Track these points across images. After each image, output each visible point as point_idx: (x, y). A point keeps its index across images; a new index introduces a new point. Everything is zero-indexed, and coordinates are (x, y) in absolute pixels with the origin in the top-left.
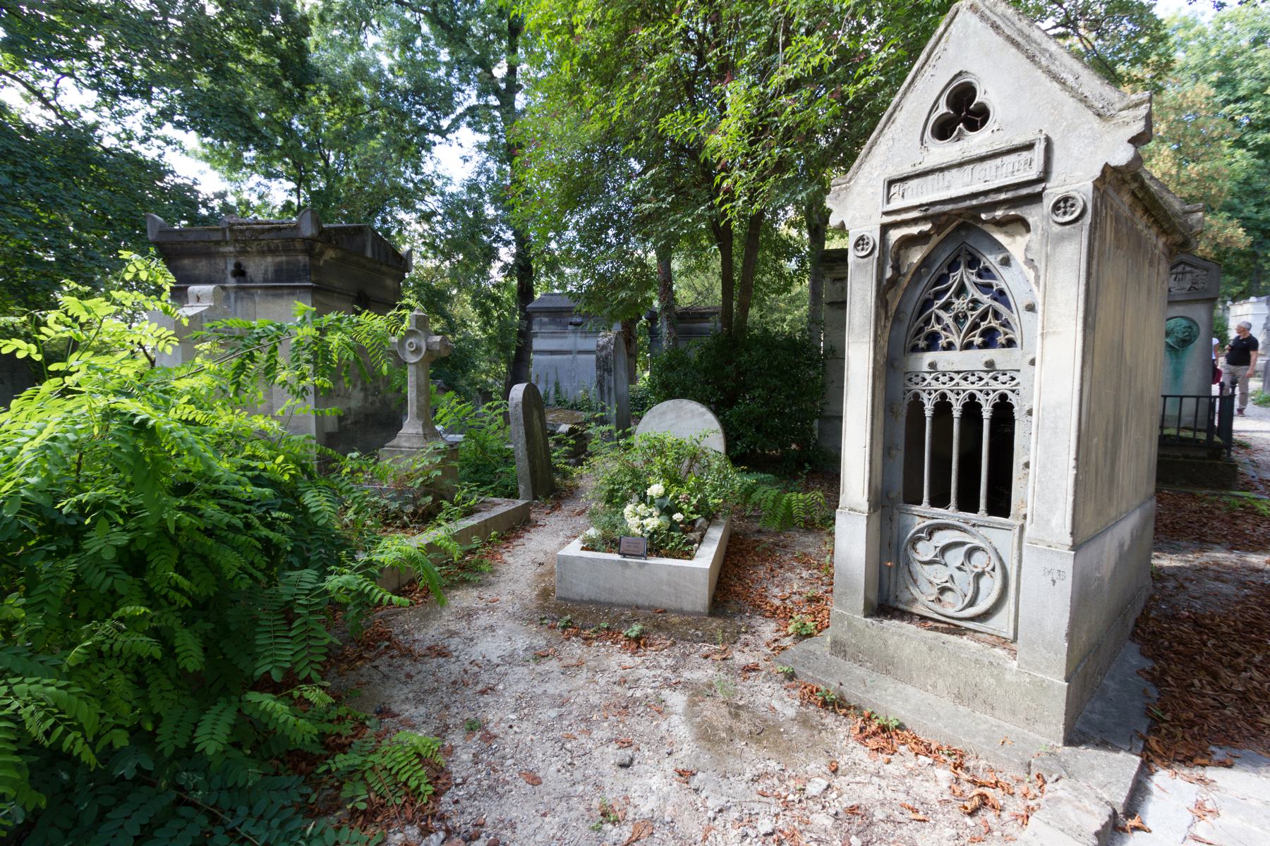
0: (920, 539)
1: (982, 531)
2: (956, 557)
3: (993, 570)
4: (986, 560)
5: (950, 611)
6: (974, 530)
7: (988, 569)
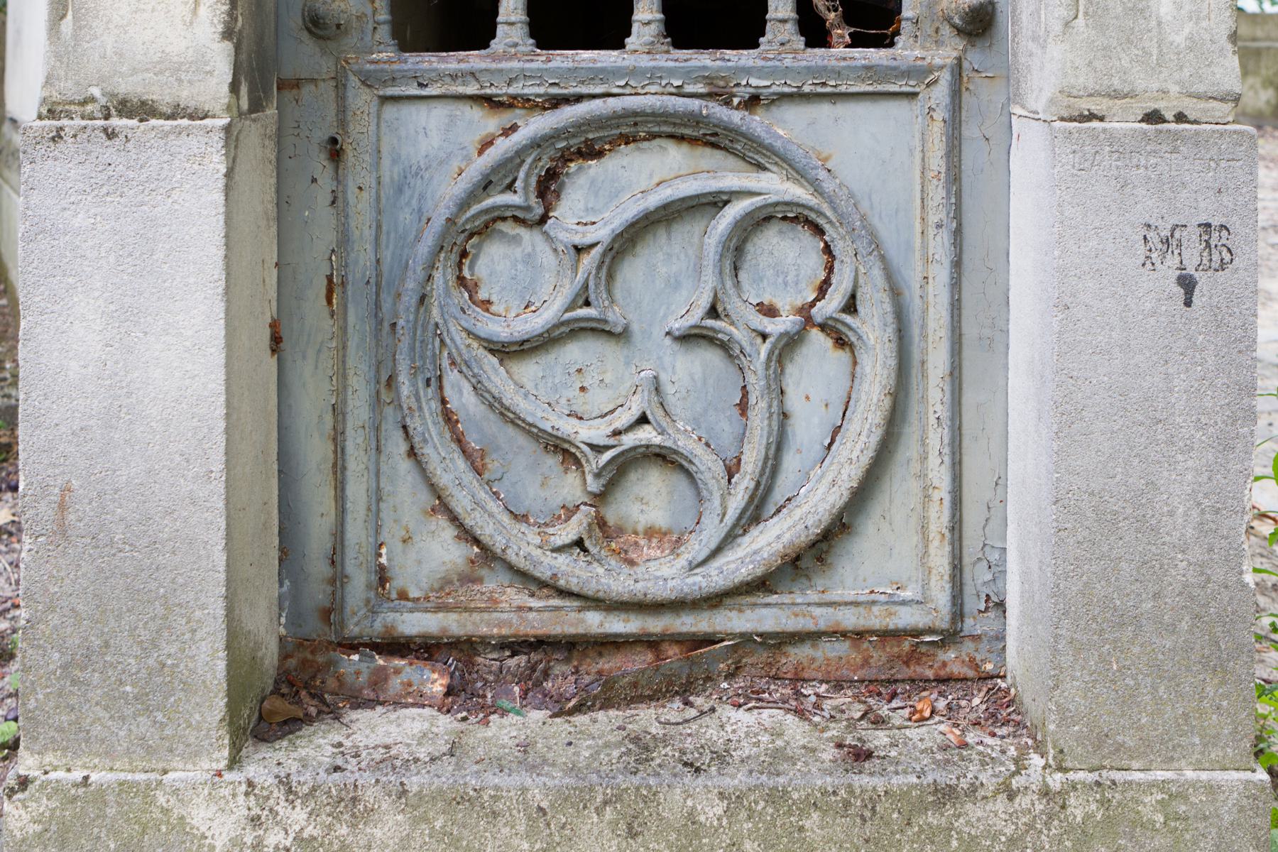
0: (487, 227)
1: (785, 126)
2: (665, 286)
3: (851, 306)
4: (813, 264)
5: (663, 574)
6: (756, 122)
7: (830, 306)
